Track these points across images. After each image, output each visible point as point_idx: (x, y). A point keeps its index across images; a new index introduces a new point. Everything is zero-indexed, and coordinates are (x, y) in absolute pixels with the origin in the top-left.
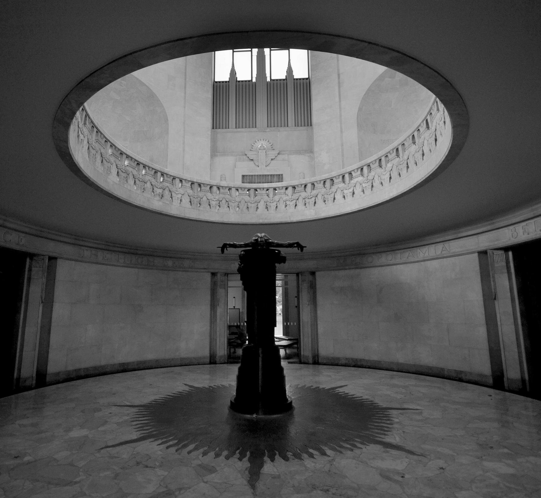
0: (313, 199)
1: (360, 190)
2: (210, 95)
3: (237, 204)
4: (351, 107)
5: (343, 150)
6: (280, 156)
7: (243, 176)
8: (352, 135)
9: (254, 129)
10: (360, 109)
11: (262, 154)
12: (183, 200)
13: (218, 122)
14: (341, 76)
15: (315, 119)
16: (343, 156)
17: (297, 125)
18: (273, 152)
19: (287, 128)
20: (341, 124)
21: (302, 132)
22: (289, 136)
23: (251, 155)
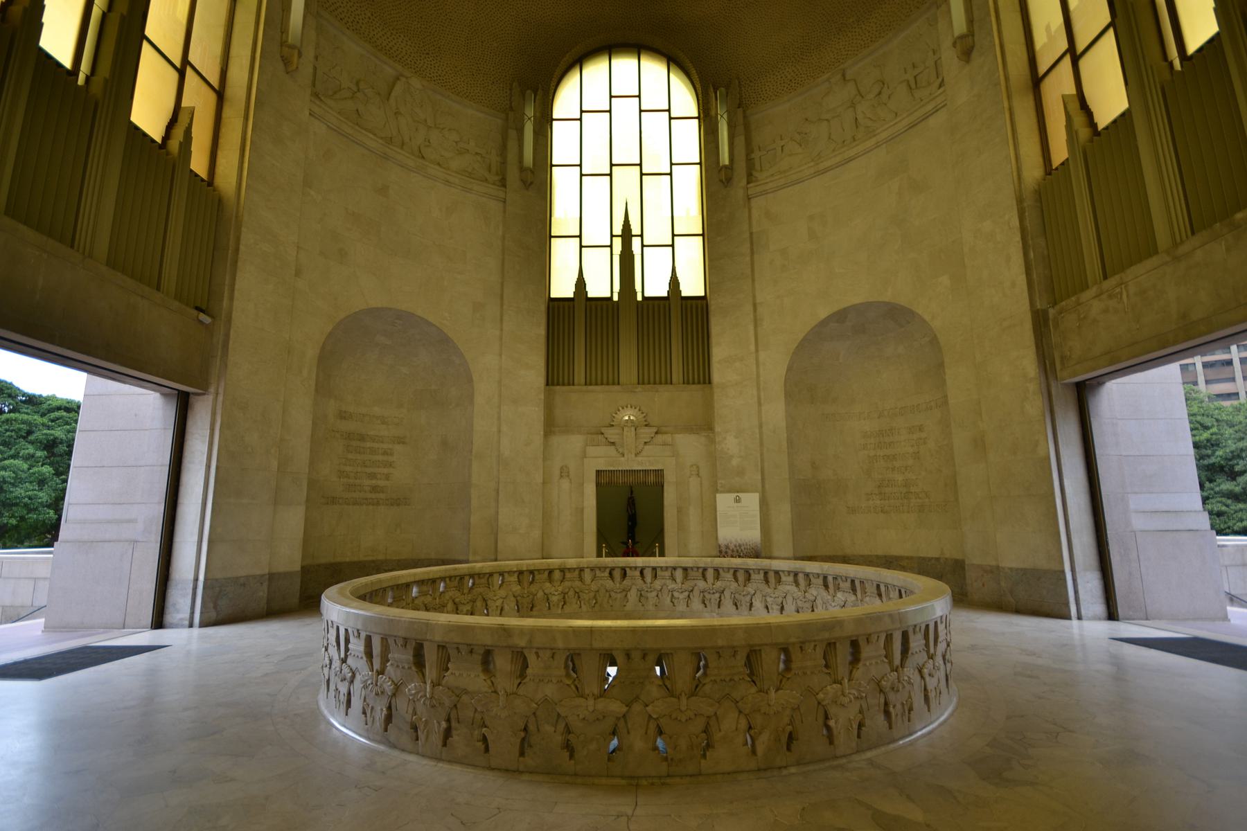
0: (717, 595)
1: (793, 608)
2: (542, 331)
3: (592, 594)
4: (775, 364)
5: (761, 434)
6: (659, 436)
7: (598, 472)
8: (776, 412)
9: (616, 388)
10: (789, 369)
11: (629, 434)
12: (506, 607)
13: (556, 376)
14: (759, 309)
15: (716, 377)
16: (761, 444)
17: (686, 382)
18: (647, 430)
19: (669, 387)
20: (758, 389)
21: (695, 392)
22: (673, 400)
23: (612, 434)
